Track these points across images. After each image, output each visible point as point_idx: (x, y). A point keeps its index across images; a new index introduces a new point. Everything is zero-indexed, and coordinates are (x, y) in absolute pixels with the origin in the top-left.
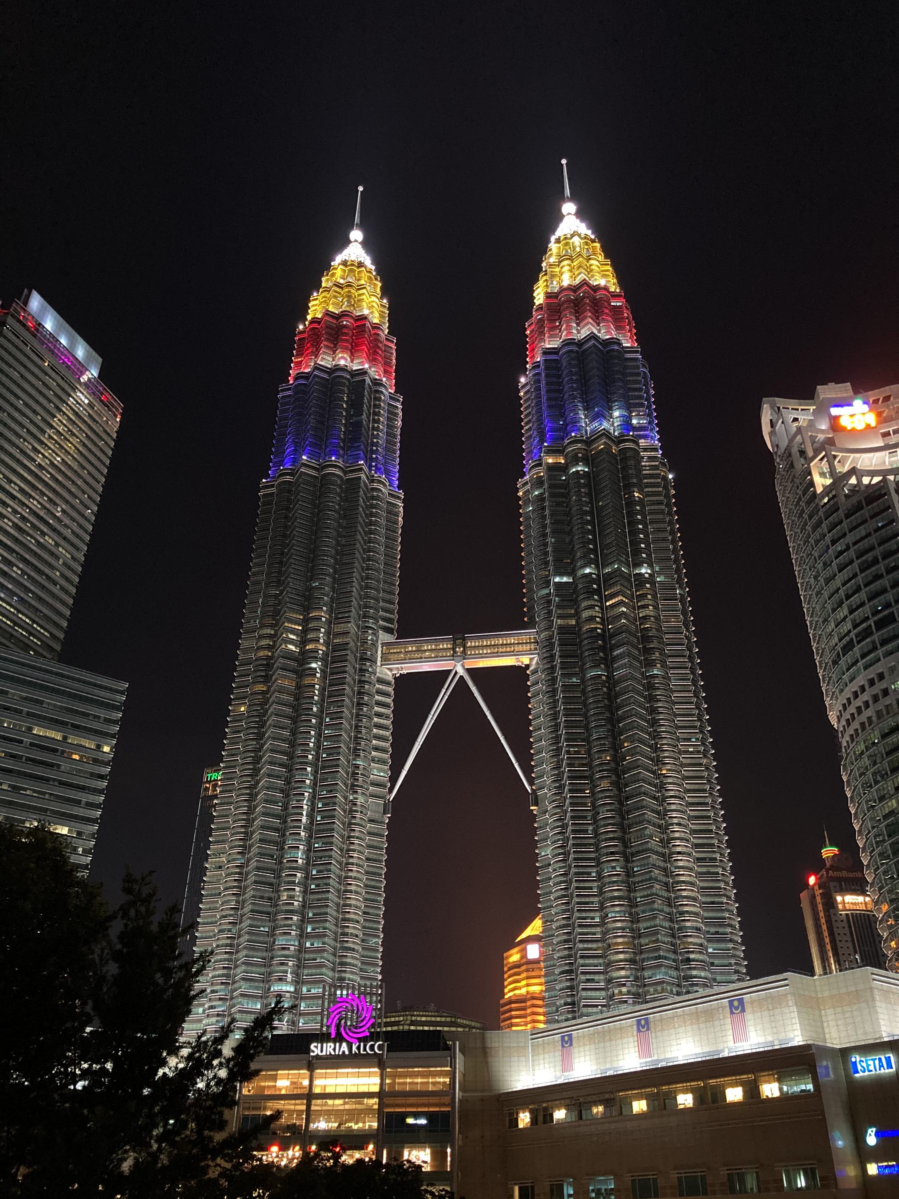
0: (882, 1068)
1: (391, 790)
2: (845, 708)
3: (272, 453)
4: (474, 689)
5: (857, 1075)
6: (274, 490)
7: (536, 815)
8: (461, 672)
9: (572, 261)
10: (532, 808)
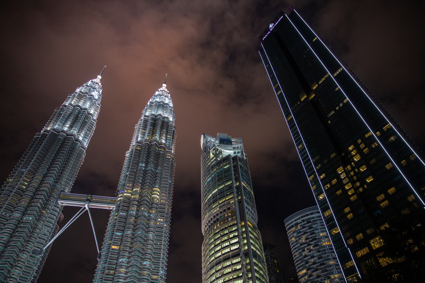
4: (89, 214)
6: (40, 136)
7: (98, 262)
8: (87, 208)
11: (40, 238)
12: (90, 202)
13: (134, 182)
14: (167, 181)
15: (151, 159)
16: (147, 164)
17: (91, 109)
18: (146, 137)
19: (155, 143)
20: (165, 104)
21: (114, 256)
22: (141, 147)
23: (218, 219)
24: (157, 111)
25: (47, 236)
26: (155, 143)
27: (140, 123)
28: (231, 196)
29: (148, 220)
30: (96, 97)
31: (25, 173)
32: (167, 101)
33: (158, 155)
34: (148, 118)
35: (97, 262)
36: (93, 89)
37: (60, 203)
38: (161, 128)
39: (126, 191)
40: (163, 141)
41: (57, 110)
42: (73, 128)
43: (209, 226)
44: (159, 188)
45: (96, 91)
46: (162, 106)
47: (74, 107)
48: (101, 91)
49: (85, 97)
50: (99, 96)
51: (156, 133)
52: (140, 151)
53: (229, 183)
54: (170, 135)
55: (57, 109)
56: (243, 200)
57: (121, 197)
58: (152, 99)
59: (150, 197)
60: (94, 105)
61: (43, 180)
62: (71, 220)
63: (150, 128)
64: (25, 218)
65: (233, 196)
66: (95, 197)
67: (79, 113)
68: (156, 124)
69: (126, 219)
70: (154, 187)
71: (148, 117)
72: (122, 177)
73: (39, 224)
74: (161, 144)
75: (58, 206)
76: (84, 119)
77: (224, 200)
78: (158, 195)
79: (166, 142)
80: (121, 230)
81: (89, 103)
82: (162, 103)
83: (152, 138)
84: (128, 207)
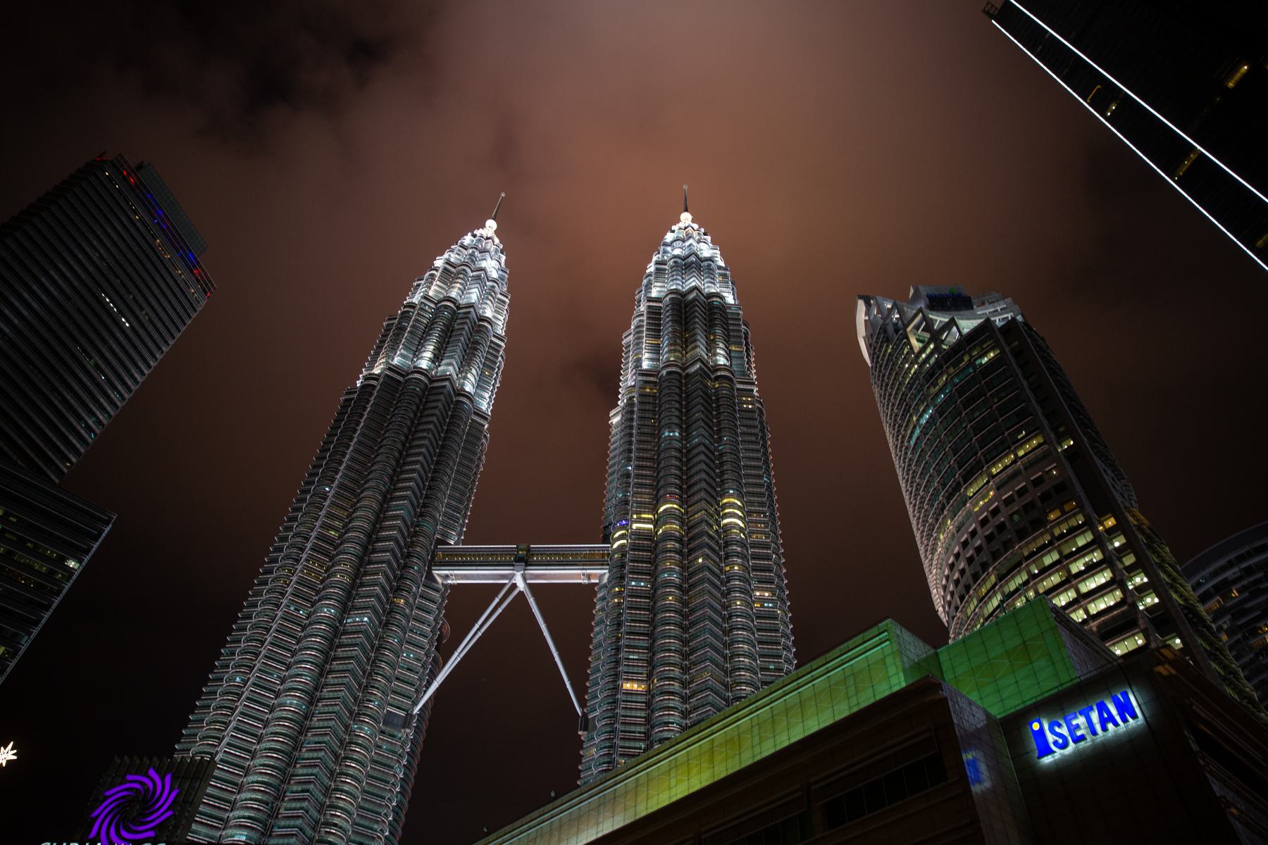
0: (1110, 726)
2: (952, 566)
3: (365, 367)
5: (1047, 760)
6: (355, 396)
7: (584, 742)
8: (521, 586)
9: (684, 242)
10: (580, 733)
11: (397, 679)
12: (526, 566)
16: (686, 430)
17: (484, 308)
19: (698, 366)
21: (633, 713)
25: (417, 673)
26: (698, 366)
29: (725, 595)
30: (494, 275)
31: (330, 495)
32: (706, 250)
34: (660, 305)
35: (580, 744)
36: (480, 252)
40: (722, 361)
41: (391, 322)
42: (448, 349)
43: (970, 560)
45: (489, 259)
47: (436, 304)
48: (503, 258)
50: (500, 272)
51: (696, 334)
54: (740, 344)
60: (492, 296)
62: (480, 622)
64: (349, 621)
70: (723, 495)
71: (661, 302)
73: (392, 637)
75: (433, 584)
76: (471, 334)
78: (739, 518)
81: (476, 290)
82: (693, 259)
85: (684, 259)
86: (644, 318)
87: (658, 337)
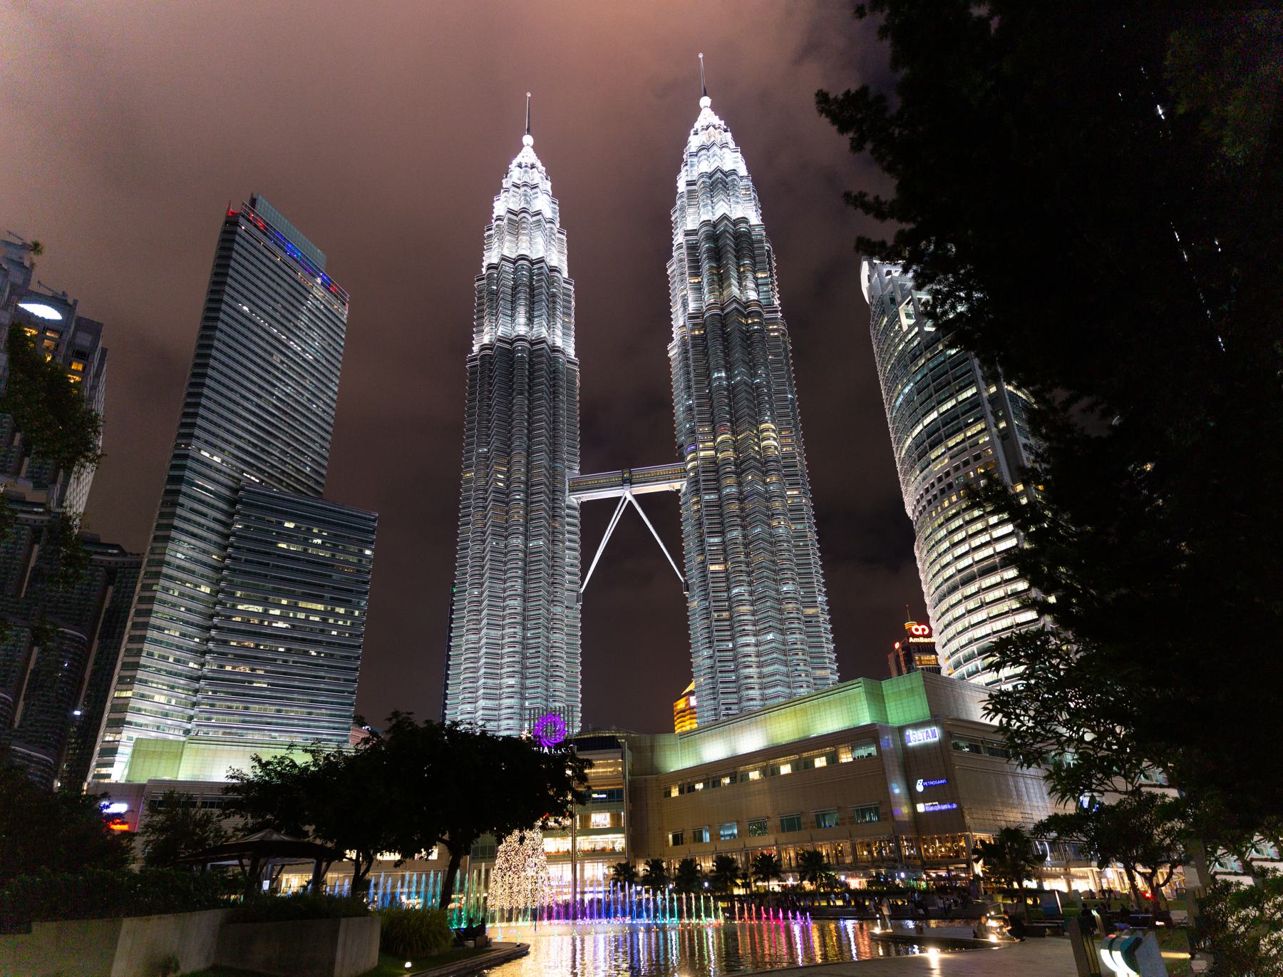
1: (581, 586)
2: (918, 501)
6: (478, 362)
8: (630, 498)
9: (708, 150)
13: (712, 422)
14: (786, 399)
15: (737, 355)
16: (729, 370)
18: (709, 298)
20: (726, 174)
22: (703, 326)
23: (950, 486)
24: (713, 208)
27: (679, 254)
28: (979, 427)
29: (768, 500)
33: (747, 336)
37: (576, 499)
38: (735, 256)
39: (701, 446)
40: (753, 295)
43: (929, 502)
44: (772, 423)
45: (540, 194)
46: (718, 183)
47: (514, 263)
49: (524, 225)
52: (703, 338)
53: (969, 393)
54: (763, 270)
55: (478, 280)
56: (1014, 431)
57: (693, 459)
58: (686, 168)
59: (757, 448)
61: (528, 463)
63: (711, 267)
65: (986, 424)
66: (638, 472)
67: (531, 278)
68: (723, 251)
69: (720, 506)
70: (762, 423)
71: (697, 234)
72: (679, 410)
74: (749, 306)
77: (959, 438)
79: (758, 295)
80: (717, 532)
82: (719, 175)
83: (721, 294)
84: (718, 480)
85: (711, 176)
86: (684, 250)
87: (697, 275)
